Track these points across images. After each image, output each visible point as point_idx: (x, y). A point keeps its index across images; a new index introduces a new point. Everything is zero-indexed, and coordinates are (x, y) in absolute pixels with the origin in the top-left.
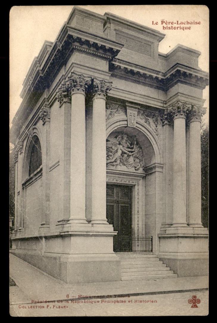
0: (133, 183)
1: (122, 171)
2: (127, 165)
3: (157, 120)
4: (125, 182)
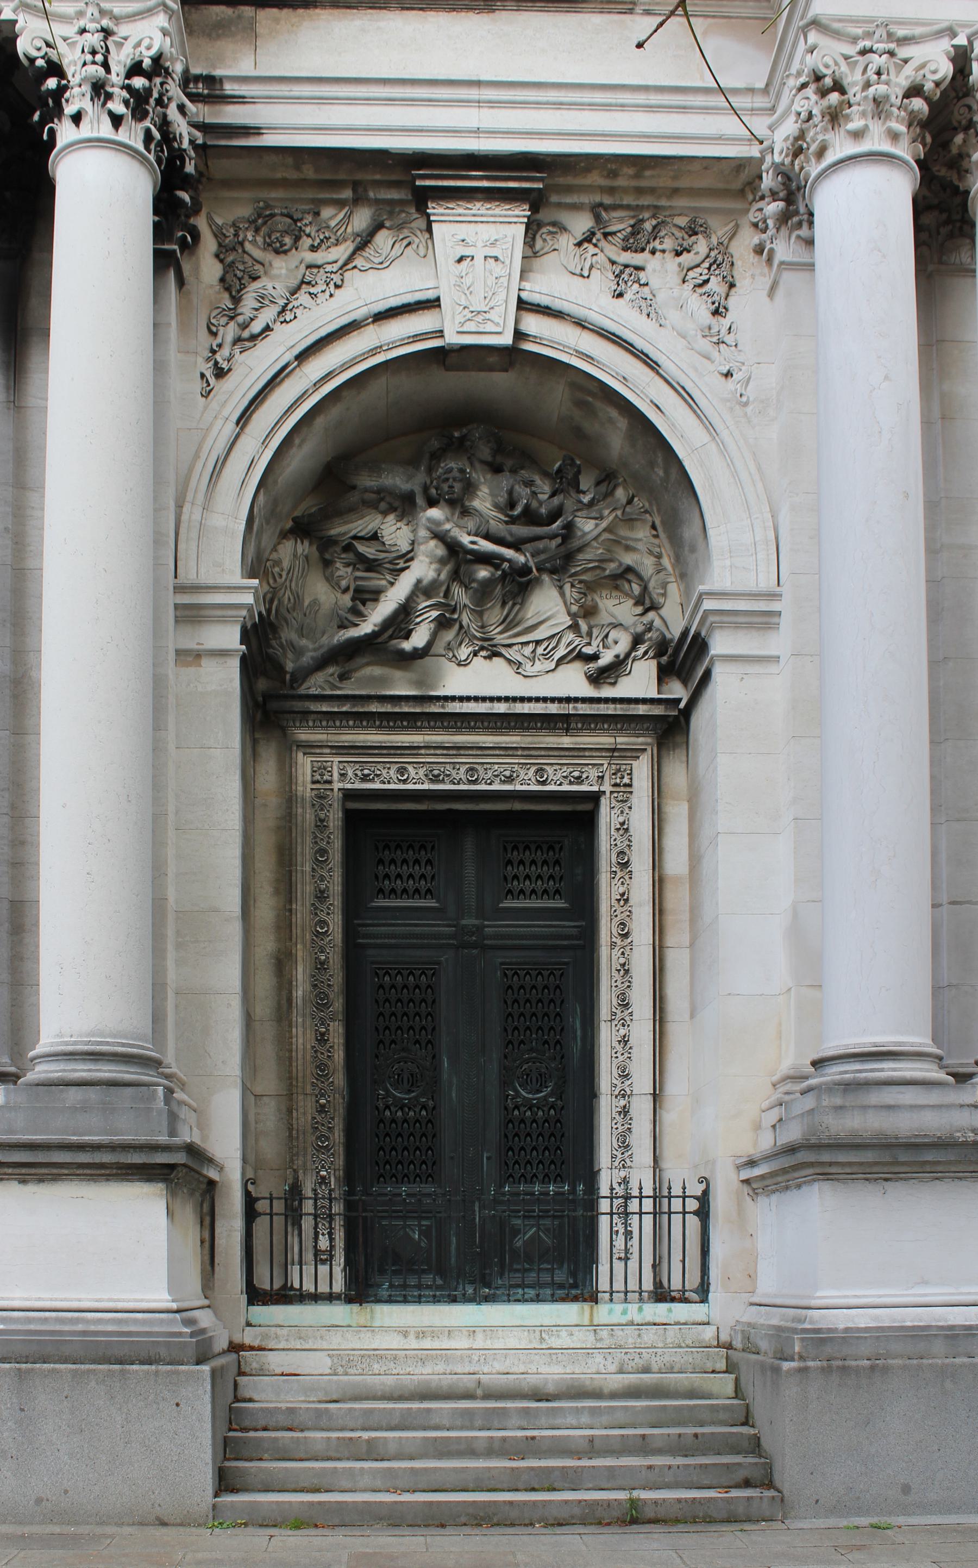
1: (476, 699)
2: (513, 654)
3: (720, 261)
4: (510, 779)
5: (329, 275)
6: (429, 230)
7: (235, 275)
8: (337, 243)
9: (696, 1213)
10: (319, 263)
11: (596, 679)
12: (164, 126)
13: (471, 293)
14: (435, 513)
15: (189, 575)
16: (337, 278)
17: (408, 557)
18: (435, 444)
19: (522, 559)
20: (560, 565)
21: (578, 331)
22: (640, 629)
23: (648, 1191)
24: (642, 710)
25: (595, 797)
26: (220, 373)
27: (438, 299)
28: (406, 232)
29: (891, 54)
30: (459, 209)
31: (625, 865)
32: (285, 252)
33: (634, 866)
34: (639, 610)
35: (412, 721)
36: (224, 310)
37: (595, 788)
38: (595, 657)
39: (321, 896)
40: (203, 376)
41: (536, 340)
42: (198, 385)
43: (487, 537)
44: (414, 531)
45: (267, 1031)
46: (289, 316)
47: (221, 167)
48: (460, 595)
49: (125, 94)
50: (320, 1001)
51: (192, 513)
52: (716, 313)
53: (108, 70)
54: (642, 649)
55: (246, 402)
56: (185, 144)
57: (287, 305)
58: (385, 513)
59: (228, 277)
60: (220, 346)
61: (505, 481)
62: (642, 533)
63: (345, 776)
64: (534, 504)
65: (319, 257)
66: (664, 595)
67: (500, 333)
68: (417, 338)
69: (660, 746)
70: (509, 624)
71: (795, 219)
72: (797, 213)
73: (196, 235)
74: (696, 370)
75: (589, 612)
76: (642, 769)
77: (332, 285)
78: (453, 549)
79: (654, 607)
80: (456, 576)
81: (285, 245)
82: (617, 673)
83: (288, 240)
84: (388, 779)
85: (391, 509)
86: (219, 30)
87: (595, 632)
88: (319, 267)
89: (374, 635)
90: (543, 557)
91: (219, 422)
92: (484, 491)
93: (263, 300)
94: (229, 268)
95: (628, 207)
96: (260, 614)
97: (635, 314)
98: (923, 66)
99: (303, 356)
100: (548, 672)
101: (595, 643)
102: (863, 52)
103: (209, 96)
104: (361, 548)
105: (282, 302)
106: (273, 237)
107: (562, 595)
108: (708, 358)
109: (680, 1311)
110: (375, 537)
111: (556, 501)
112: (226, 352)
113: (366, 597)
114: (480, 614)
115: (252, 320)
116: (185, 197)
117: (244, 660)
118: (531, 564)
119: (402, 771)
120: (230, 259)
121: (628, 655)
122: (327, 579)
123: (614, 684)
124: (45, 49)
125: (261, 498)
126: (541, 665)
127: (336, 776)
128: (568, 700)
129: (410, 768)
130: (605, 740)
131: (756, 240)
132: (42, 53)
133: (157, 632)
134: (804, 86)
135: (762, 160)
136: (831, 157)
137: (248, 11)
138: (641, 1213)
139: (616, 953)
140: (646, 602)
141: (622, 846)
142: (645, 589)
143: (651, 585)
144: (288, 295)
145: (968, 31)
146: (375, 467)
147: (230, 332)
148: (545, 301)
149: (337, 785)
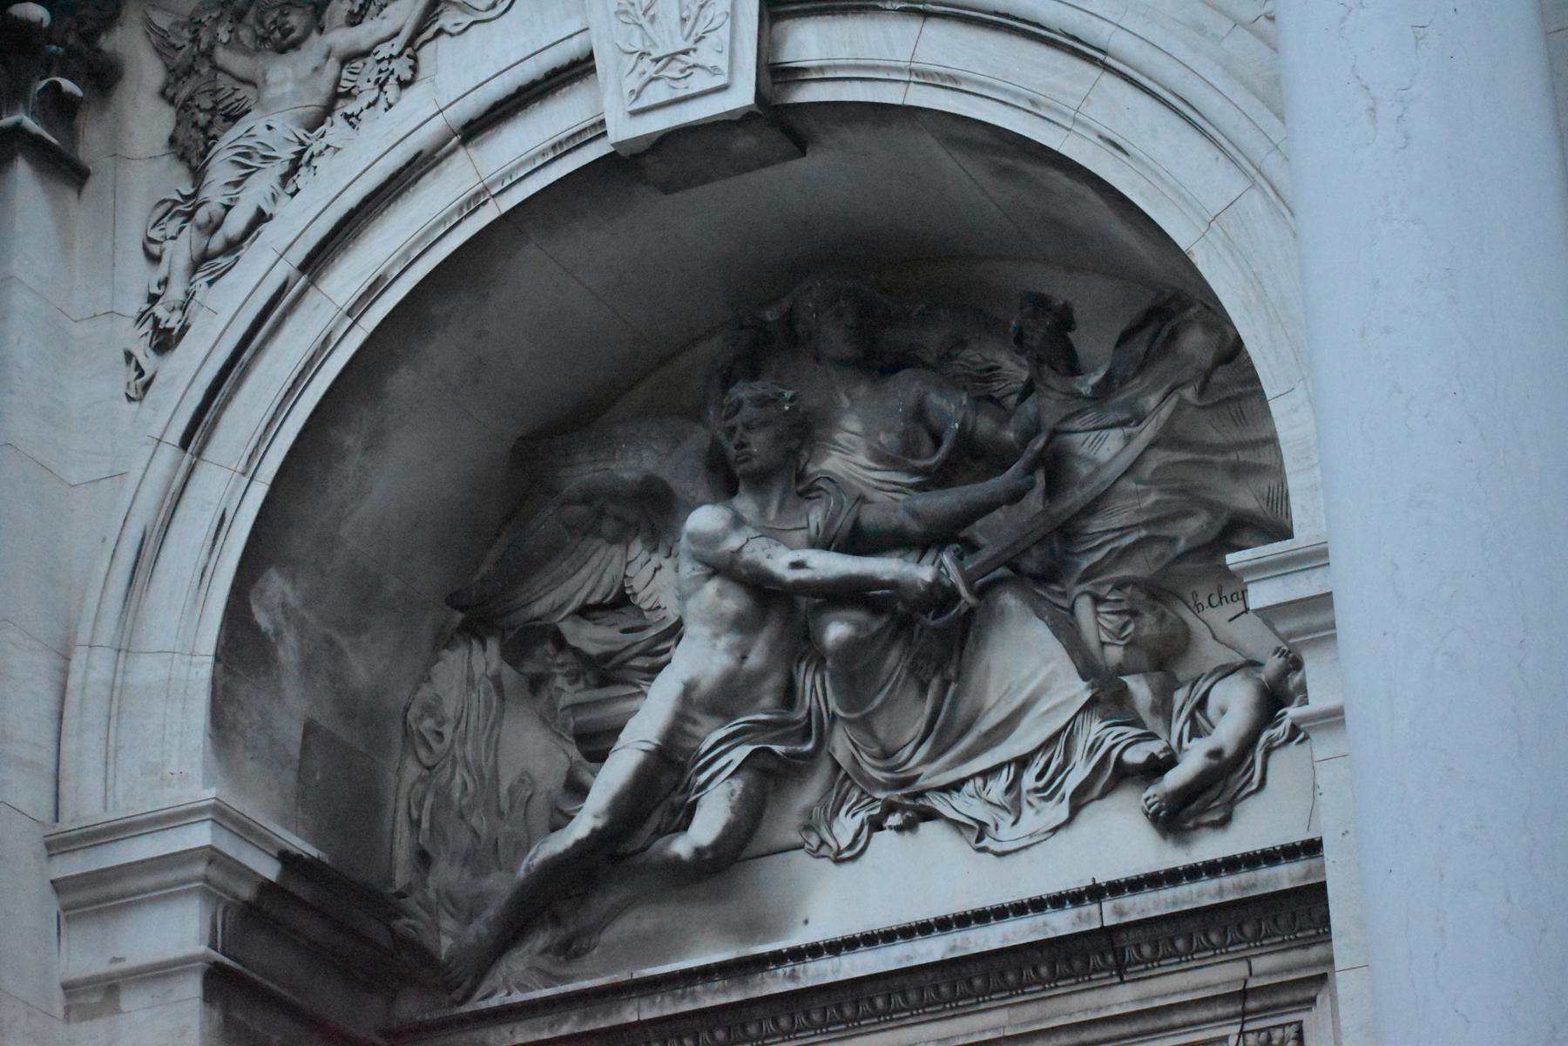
5: (384, 65)
7: (195, 124)
10: (364, 45)
11: (1174, 818)
13: (653, 19)
32: (295, 45)
36: (176, 203)
41: (822, 75)
57: (303, 152)
60: (164, 282)
65: (363, 35)
67: (725, 88)
77: (392, 88)
78: (764, 592)
81: (292, 30)
82: (1228, 795)
88: (366, 54)
100: (1055, 830)
105: (287, 153)
106: (268, 21)
115: (228, 208)
118: (955, 577)
123: (1224, 823)
144: (301, 133)
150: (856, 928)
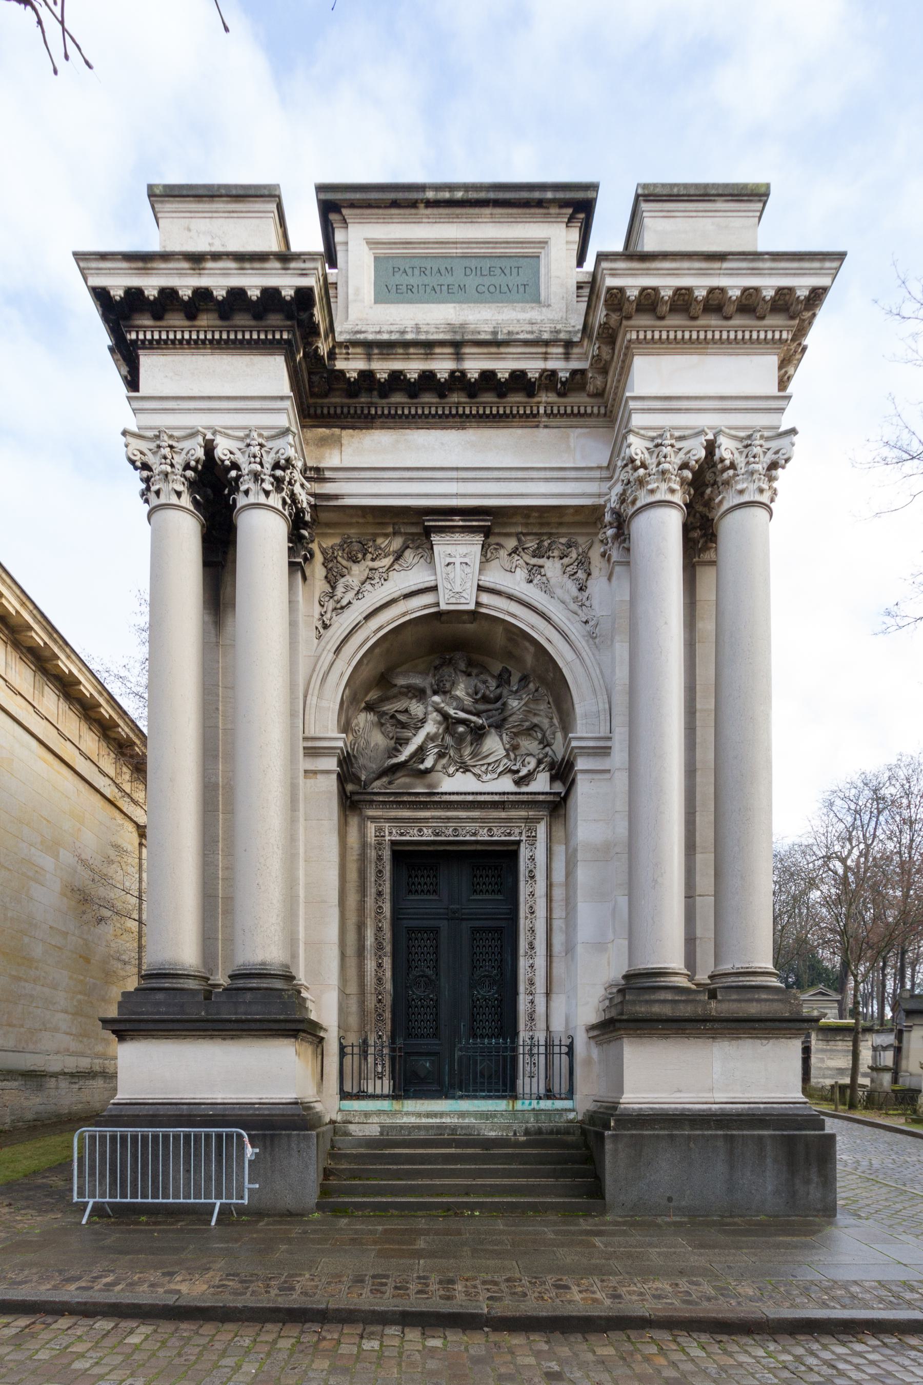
0: (509, 834)
1: (457, 793)
2: (476, 770)
3: (584, 562)
4: (475, 834)
6: (432, 549)
8: (385, 557)
9: (566, 1054)
11: (517, 783)
12: (293, 495)
14: (436, 699)
15: (311, 733)
16: (385, 575)
17: (423, 721)
18: (437, 662)
19: (481, 721)
20: (499, 726)
21: (509, 601)
22: (541, 756)
23: (542, 1042)
24: (541, 798)
25: (518, 843)
26: (326, 627)
27: (436, 586)
28: (420, 550)
29: (672, 446)
30: (447, 537)
31: (532, 877)
32: (358, 562)
33: (538, 878)
34: (541, 746)
35: (425, 805)
37: (518, 838)
38: (518, 771)
39: (380, 894)
40: (317, 628)
42: (314, 633)
43: (463, 710)
44: (426, 708)
45: (352, 962)
46: (360, 596)
47: (324, 516)
48: (449, 740)
49: (272, 480)
50: (379, 947)
51: (312, 700)
52: (581, 589)
53: (262, 466)
54: (542, 766)
55: (339, 643)
56: (305, 505)
58: (411, 698)
59: (329, 576)
61: (474, 681)
62: (543, 707)
63: (391, 834)
64: (488, 692)
65: (376, 564)
66: (554, 738)
68: (426, 607)
69: (551, 816)
70: (474, 755)
71: (622, 538)
72: (623, 534)
73: (312, 555)
74: (569, 620)
75: (515, 748)
76: (541, 830)
78: (446, 716)
79: (549, 745)
80: (447, 730)
83: (360, 556)
84: (413, 835)
85: (415, 696)
86: (323, 442)
87: (518, 758)
89: (406, 762)
90: (491, 720)
91: (325, 652)
92: (462, 686)
93: (347, 588)
94: (329, 570)
95: (535, 534)
96: (347, 752)
97: (538, 591)
98: (689, 452)
99: (367, 618)
101: (518, 764)
102: (657, 446)
103: (317, 478)
104: (400, 717)
107: (502, 739)
108: (576, 614)
109: (559, 1104)
110: (406, 711)
111: (499, 691)
112: (328, 615)
113: (402, 742)
114: (460, 750)
116: (305, 533)
117: (339, 775)
118: (485, 724)
119: (420, 830)
120: (330, 566)
121: (535, 770)
122: (383, 733)
123: (527, 785)
124: (229, 455)
125: (347, 691)
126: (489, 776)
127: (387, 833)
128: (504, 793)
129: (424, 829)
130: (523, 813)
131: (602, 550)
132: (227, 457)
133: (293, 760)
134: (626, 465)
135: (605, 506)
136: (639, 504)
137: (337, 431)
138: (538, 1054)
139: (528, 921)
140: (545, 743)
141: (531, 867)
142: (544, 736)
143: (548, 733)
145: (714, 431)
146: (405, 673)
147: (331, 605)
148: (491, 586)
149: (387, 838)
150: (455, 790)
